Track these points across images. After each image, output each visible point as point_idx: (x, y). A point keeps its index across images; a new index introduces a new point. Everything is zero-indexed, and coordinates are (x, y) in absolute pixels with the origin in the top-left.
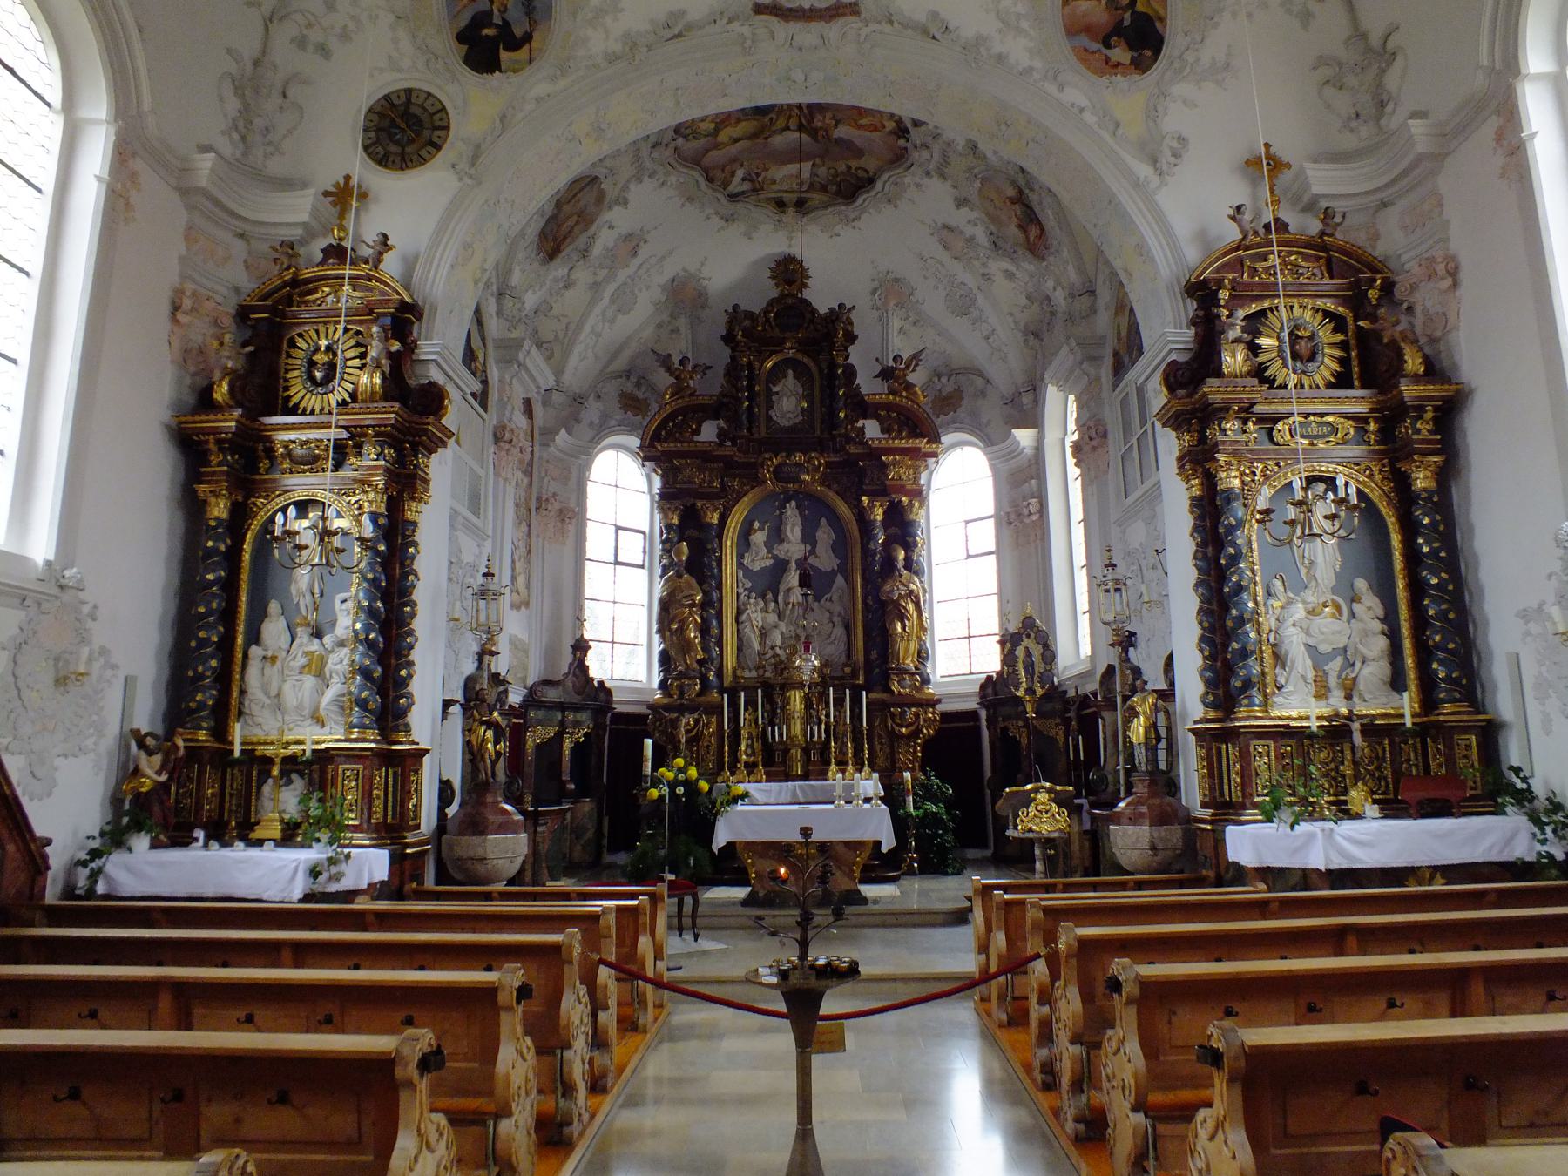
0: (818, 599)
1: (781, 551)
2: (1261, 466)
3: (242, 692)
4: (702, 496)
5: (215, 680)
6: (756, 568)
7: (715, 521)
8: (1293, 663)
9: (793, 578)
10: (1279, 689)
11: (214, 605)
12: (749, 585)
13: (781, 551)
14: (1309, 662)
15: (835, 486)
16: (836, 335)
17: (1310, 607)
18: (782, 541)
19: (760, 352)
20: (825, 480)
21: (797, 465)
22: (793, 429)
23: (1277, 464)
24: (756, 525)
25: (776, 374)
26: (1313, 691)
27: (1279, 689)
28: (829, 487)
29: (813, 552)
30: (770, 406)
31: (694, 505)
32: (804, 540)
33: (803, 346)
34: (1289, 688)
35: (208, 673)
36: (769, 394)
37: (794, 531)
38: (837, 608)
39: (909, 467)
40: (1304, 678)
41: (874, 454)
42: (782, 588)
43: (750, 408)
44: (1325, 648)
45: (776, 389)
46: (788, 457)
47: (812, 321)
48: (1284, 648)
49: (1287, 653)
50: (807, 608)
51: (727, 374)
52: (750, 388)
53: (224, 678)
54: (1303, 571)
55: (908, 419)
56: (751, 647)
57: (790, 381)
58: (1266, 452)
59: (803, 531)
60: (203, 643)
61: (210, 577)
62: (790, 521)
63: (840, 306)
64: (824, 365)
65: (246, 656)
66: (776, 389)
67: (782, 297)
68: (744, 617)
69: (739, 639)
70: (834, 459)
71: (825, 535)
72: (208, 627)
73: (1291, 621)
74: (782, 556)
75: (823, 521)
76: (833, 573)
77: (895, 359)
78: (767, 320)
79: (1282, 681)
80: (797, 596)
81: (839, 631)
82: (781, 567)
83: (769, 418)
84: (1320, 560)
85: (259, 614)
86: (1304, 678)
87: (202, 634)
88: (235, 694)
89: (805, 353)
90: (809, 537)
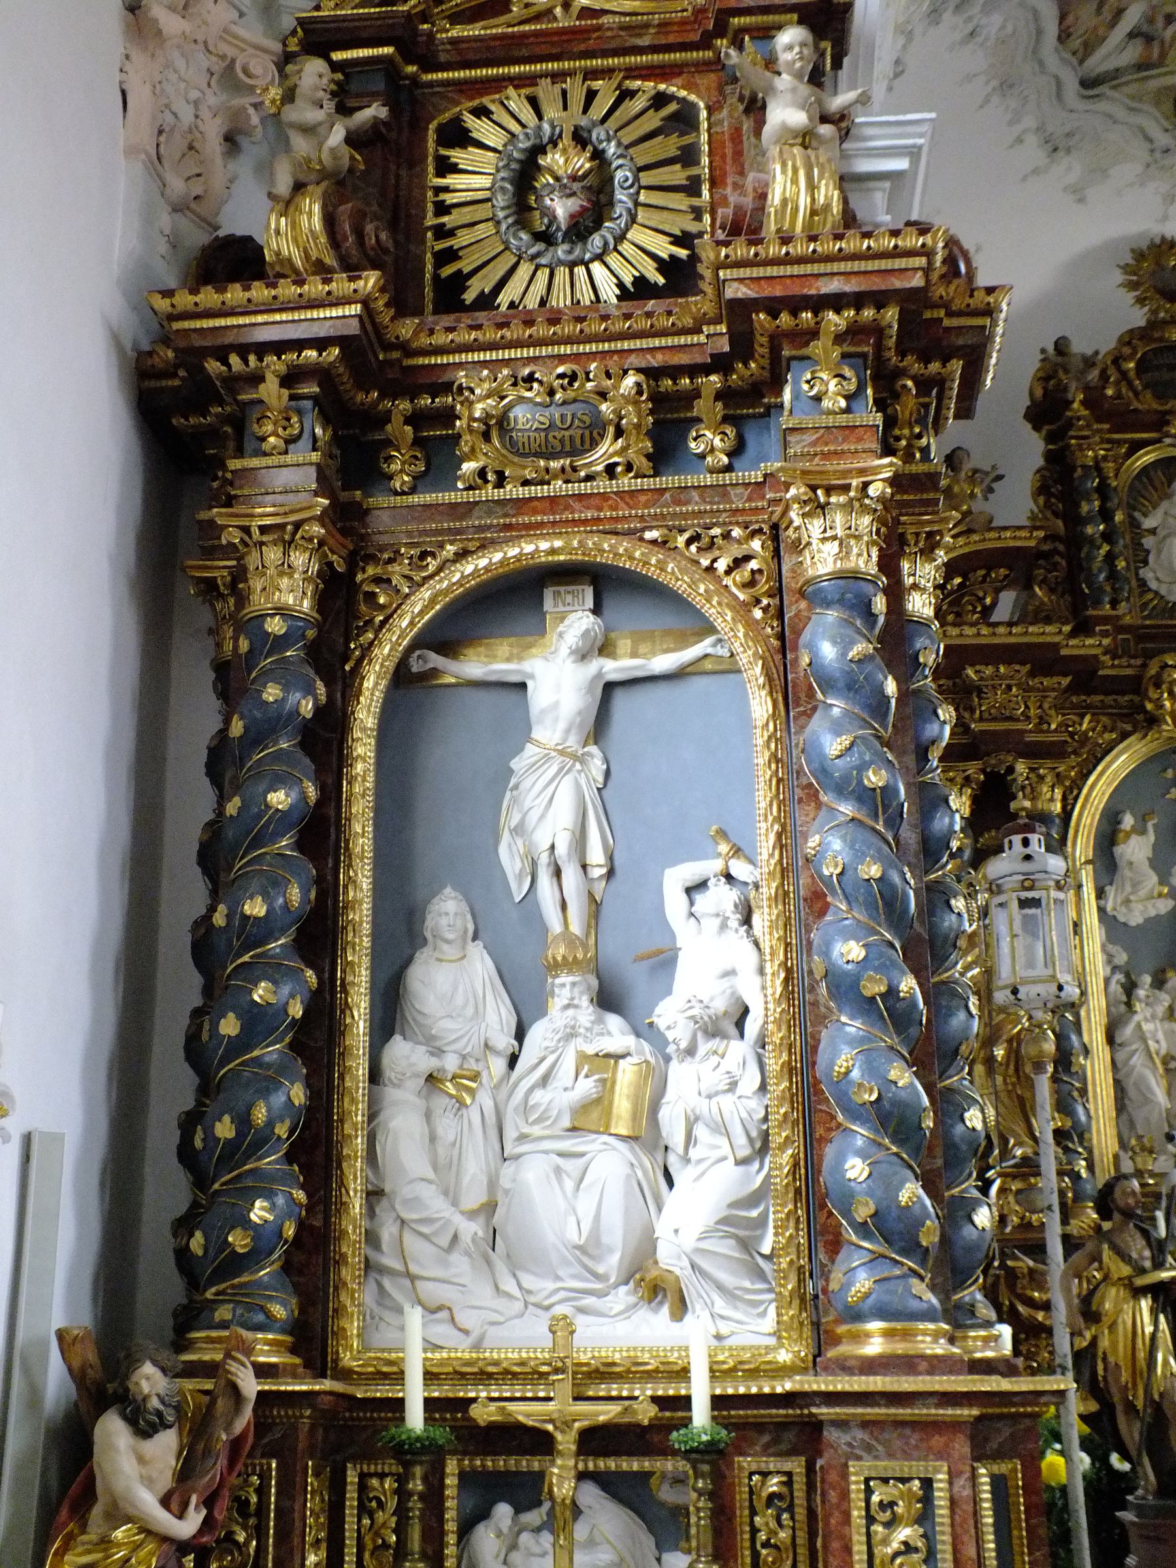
3: (374, 1195)
4: (1034, 752)
5: (289, 1158)
6: (1135, 918)
7: (1057, 807)
11: (295, 894)
12: (1122, 958)
24: (1128, 821)
31: (1011, 770)
35: (282, 1130)
43: (1110, 558)
45: (1148, 523)
51: (1042, 490)
52: (1106, 515)
53: (316, 1150)
56: (1147, 1100)
60: (259, 1023)
61: (279, 799)
65: (375, 1076)
67: (1153, 324)
68: (1128, 1032)
69: (1117, 1082)
72: (273, 970)
78: (1124, 374)
85: (401, 937)
87: (261, 993)
88: (357, 1205)
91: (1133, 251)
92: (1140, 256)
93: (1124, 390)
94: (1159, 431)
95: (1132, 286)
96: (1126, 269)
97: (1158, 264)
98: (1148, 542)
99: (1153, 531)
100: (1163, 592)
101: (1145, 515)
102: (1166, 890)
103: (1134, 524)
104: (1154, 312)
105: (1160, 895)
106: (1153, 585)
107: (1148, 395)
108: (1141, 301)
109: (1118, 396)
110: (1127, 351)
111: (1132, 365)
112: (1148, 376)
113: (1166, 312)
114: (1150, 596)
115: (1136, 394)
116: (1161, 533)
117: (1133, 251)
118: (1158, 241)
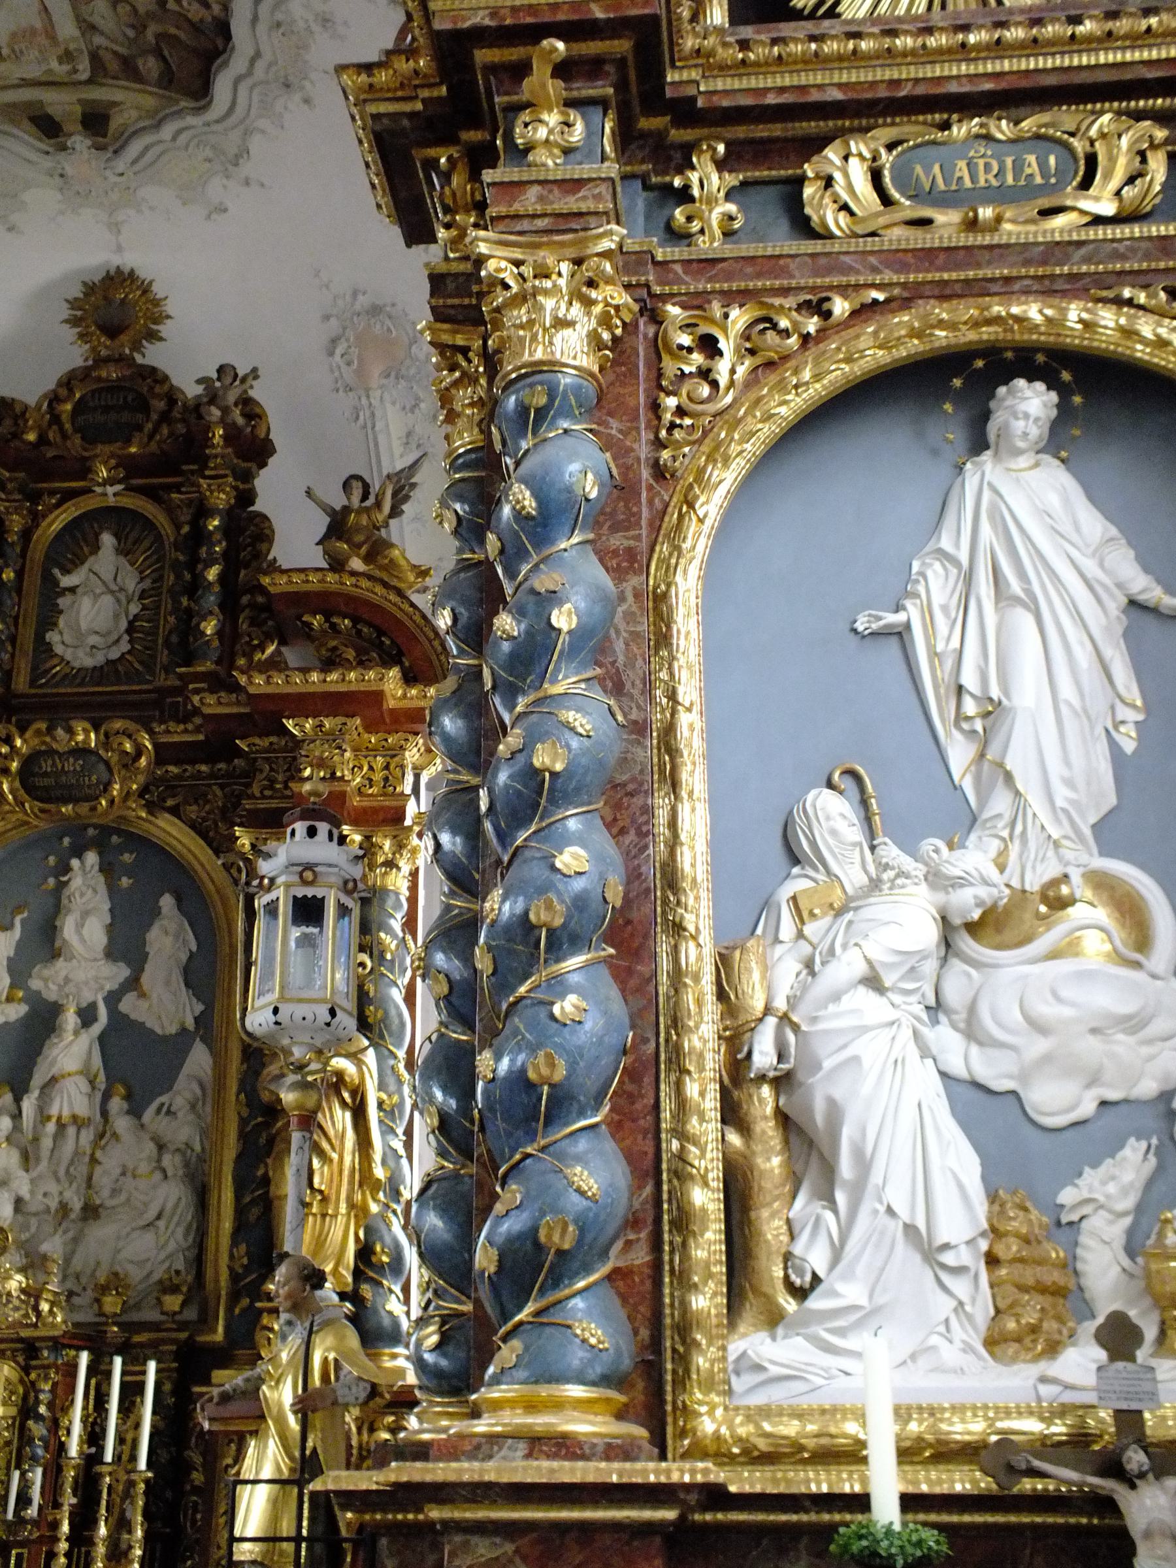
0: (135, 1111)
1: (48, 981)
2: (739, 318)
8: (864, 1165)
9: (72, 1052)
10: (800, 1293)
13: (48, 981)
14: (959, 1163)
15: (192, 811)
16: (207, 442)
17: (967, 902)
18: (54, 954)
19: (34, 497)
20: (155, 796)
21: (82, 752)
22: (107, 671)
23: (820, 308)
25: (75, 545)
26: (982, 1308)
27: (800, 1293)
28: (175, 811)
29: (133, 983)
30: (48, 618)
32: (111, 954)
33: (131, 471)
34: (844, 1291)
36: (51, 593)
37: (86, 927)
38: (183, 1131)
39: (372, 751)
40: (930, 1251)
41: (268, 715)
42: (37, 1080)
44: (1057, 1099)
45: (66, 581)
46: (50, 730)
47: (165, 417)
48: (820, 1091)
49: (835, 1113)
50: (104, 1134)
54: (960, 753)
55: (381, 632)
57: (107, 557)
58: (773, 264)
59: (110, 929)
62: (78, 903)
63: (221, 370)
64: (185, 516)
66: (66, 581)
67: (100, 362)
70: (178, 734)
71: (168, 939)
73: (847, 966)
74: (51, 993)
75: (167, 902)
76: (180, 1043)
77: (346, 486)
78: (56, 419)
79: (816, 1258)
80: (73, 1099)
81: (173, 1194)
82: (42, 1021)
83: (43, 649)
84: (1028, 694)
86: (930, 1251)
89: (150, 493)
90: (126, 945)
91: (85, 284)
92: (90, 289)
93: (51, 435)
94: (84, 479)
95: (74, 322)
96: (73, 304)
97: (105, 298)
98: (63, 602)
99: (72, 590)
100: (68, 657)
101: (66, 571)
102: (21, 994)
103: (50, 582)
104: (93, 349)
105: (9, 999)
106: (59, 649)
107: (77, 440)
108: (81, 336)
109: (43, 440)
110: (63, 392)
111: (69, 407)
112: (80, 420)
113: (106, 347)
114: (55, 661)
115: (65, 436)
116: (79, 590)
117: (85, 284)
118: (112, 273)
